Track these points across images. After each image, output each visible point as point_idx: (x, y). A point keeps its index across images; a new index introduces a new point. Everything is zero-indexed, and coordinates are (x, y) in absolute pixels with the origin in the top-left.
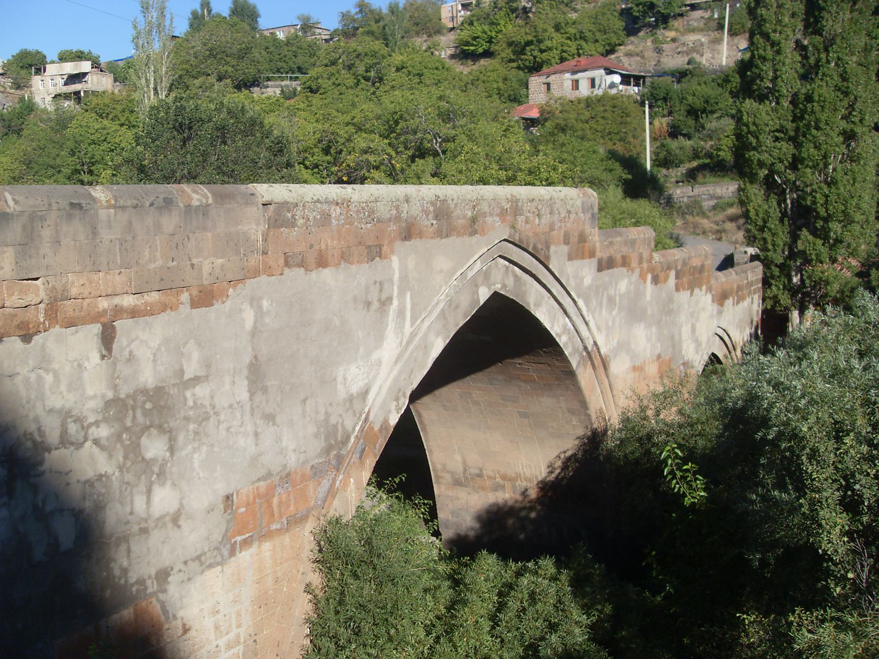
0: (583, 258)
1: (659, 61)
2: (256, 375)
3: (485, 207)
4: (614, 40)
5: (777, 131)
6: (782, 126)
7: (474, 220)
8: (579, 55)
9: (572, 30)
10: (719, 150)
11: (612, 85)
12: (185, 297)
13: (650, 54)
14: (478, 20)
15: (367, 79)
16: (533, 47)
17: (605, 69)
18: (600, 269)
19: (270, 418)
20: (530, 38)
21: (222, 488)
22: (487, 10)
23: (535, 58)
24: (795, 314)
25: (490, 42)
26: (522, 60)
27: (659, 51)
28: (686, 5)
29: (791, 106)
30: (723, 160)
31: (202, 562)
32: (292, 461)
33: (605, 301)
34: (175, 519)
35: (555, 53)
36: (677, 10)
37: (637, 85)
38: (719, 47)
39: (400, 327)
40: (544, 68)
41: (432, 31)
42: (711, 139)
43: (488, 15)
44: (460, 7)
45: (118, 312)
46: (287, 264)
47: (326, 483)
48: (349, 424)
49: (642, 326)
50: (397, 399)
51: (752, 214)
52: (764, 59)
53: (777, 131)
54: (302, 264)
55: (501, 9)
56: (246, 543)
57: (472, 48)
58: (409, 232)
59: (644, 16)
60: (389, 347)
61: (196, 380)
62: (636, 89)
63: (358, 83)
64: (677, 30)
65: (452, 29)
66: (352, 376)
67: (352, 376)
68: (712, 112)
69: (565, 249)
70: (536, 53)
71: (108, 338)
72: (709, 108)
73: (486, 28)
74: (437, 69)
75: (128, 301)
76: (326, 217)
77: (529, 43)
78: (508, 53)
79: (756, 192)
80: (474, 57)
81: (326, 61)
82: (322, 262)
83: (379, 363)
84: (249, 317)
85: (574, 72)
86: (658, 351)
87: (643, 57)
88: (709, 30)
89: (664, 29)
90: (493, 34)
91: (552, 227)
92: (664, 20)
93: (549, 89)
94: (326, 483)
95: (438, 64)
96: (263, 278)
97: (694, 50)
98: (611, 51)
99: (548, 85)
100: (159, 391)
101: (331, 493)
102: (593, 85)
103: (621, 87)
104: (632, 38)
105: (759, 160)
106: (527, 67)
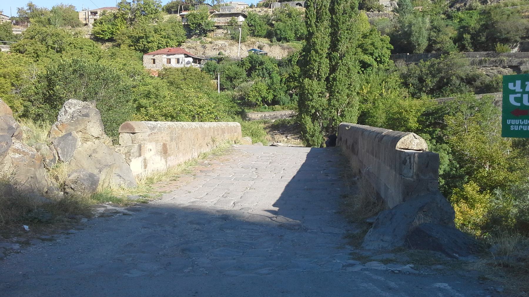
1: (204, 52)
4: (181, 40)
5: (320, 93)
6: (322, 91)
8: (167, 46)
9: (163, 33)
10: (249, 97)
11: (188, 63)
13: (199, 48)
14: (105, 22)
15: (53, 48)
16: (143, 40)
17: (185, 54)
20: (142, 35)
22: (110, 17)
23: (144, 45)
25: (112, 34)
26: (137, 46)
27: (204, 47)
28: (215, 26)
29: (326, 82)
30: (251, 102)
35: (155, 44)
36: (211, 28)
37: (200, 63)
38: (235, 48)
40: (150, 51)
41: (74, 25)
42: (242, 91)
43: (110, 20)
44: (90, 14)
51: (308, 129)
52: (316, 61)
53: (320, 93)
55: (118, 17)
57: (102, 36)
59: (196, 29)
62: (199, 65)
63: (48, 51)
64: (211, 37)
65: (86, 24)
68: (238, 78)
70: (145, 43)
72: (237, 77)
73: (110, 26)
74: (90, 46)
77: (142, 38)
78: (129, 41)
79: (308, 119)
80: (103, 41)
81: (28, 36)
85: (168, 55)
87: (196, 49)
88: (227, 39)
89: (205, 36)
90: (114, 30)
92: (204, 32)
93: (154, 63)
95: (91, 44)
97: (221, 48)
98: (179, 45)
99: (154, 60)
102: (178, 62)
103: (193, 64)
104: (189, 40)
105: (312, 105)
106: (139, 50)
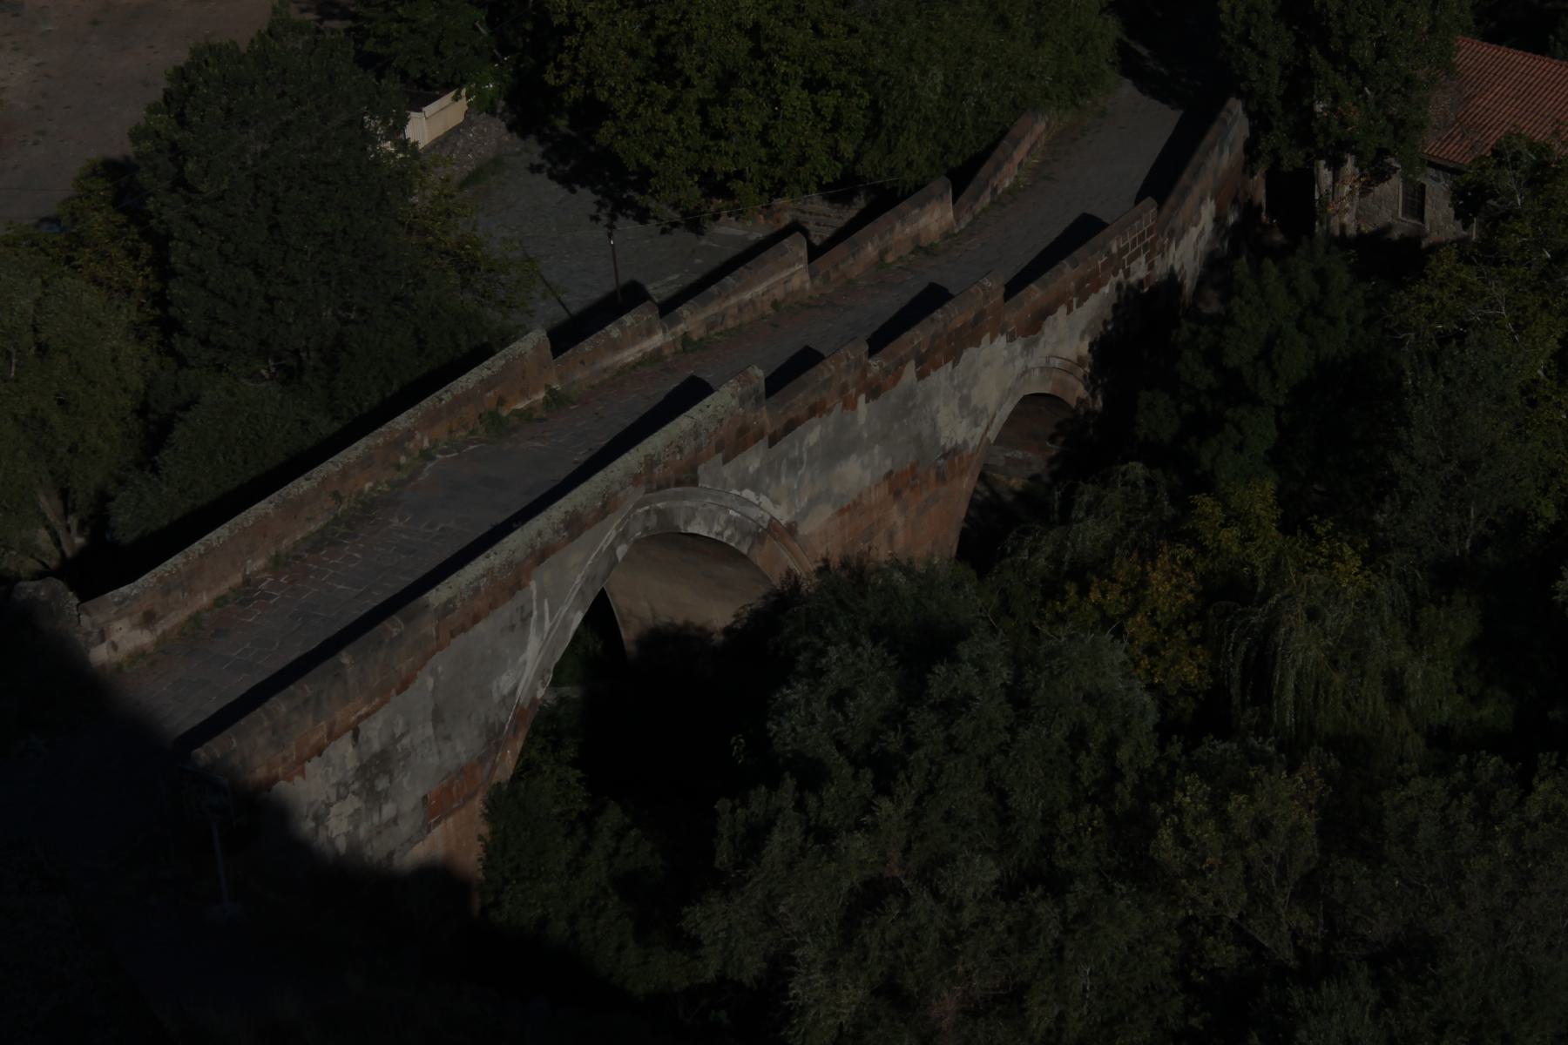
0: (745, 449)
2: (437, 717)
3: (617, 487)
7: (604, 506)
12: (393, 692)
18: (773, 441)
19: (448, 738)
21: (420, 793)
24: (1325, 175)
31: (411, 842)
32: (464, 759)
33: (784, 468)
34: (395, 821)
39: (540, 628)
45: (360, 719)
46: (453, 636)
47: (489, 765)
48: (503, 718)
49: (853, 457)
50: (542, 677)
54: (464, 629)
56: (437, 823)
58: (541, 555)
60: (534, 644)
61: (403, 735)
66: (505, 683)
67: (505, 683)
69: (720, 456)
71: (355, 737)
75: (364, 710)
76: (477, 589)
82: (476, 619)
83: (525, 663)
84: (430, 683)
86: (888, 463)
91: (698, 449)
94: (489, 765)
96: (438, 654)
100: (383, 751)
101: (494, 768)
